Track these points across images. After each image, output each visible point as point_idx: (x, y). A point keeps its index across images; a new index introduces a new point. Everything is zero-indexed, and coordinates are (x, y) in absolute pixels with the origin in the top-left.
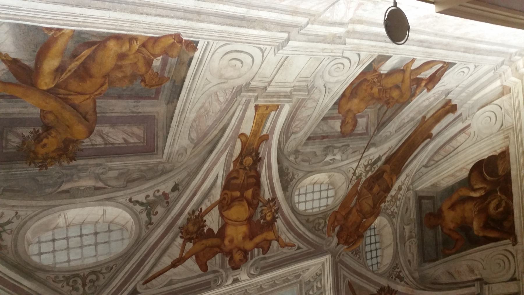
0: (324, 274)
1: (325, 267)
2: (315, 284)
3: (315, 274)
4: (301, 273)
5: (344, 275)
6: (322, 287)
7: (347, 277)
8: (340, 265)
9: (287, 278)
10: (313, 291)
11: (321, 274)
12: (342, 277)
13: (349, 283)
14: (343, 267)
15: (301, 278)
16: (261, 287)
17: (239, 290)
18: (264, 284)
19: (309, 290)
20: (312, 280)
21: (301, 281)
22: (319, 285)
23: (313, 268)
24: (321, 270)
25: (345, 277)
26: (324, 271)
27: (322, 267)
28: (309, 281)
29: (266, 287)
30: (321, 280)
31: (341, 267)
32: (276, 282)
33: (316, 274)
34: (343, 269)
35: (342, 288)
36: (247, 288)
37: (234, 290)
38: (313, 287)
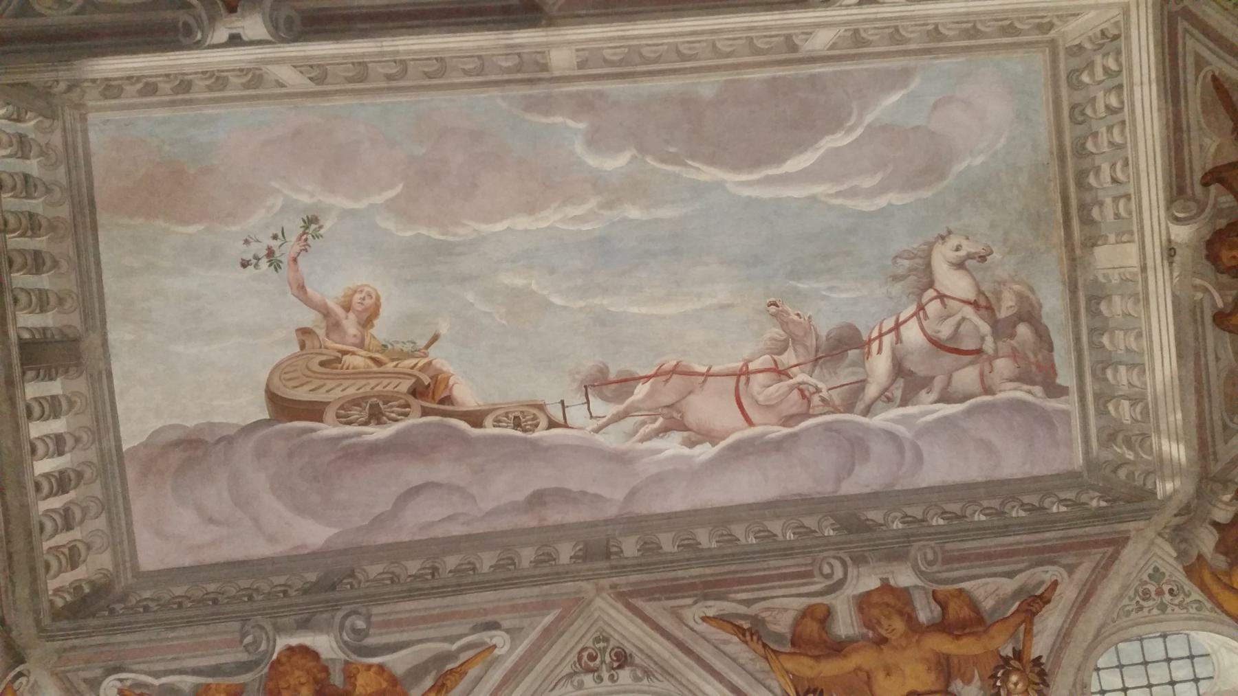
0: (1128, 37)
1: (1134, 18)
2: (1098, 59)
3: (1099, 29)
4: (1055, 20)
5: (1198, 56)
6: (1120, 71)
7: (1208, 63)
8: (1182, 25)
9: (1011, 25)
10: (1092, 74)
11: (1116, 37)
12: (1190, 60)
13: (1215, 79)
14: (1196, 32)
15: (1052, 34)
16: (936, 28)
17: (879, 25)
18: (943, 25)
19: (1079, 71)
20: (1088, 46)
21: (1053, 42)
22: (1113, 66)
23: (1092, 13)
24: (1116, 24)
25: (1200, 63)
26: (1128, 29)
27: (1120, 18)
28: (1080, 47)
29: (951, 33)
30: (1119, 53)
31: (1186, 30)
32: (979, 26)
33: (1103, 33)
34: (1192, 35)
35: (1190, 88)
36: (898, 23)
37: (865, 21)
38: (1090, 65)
